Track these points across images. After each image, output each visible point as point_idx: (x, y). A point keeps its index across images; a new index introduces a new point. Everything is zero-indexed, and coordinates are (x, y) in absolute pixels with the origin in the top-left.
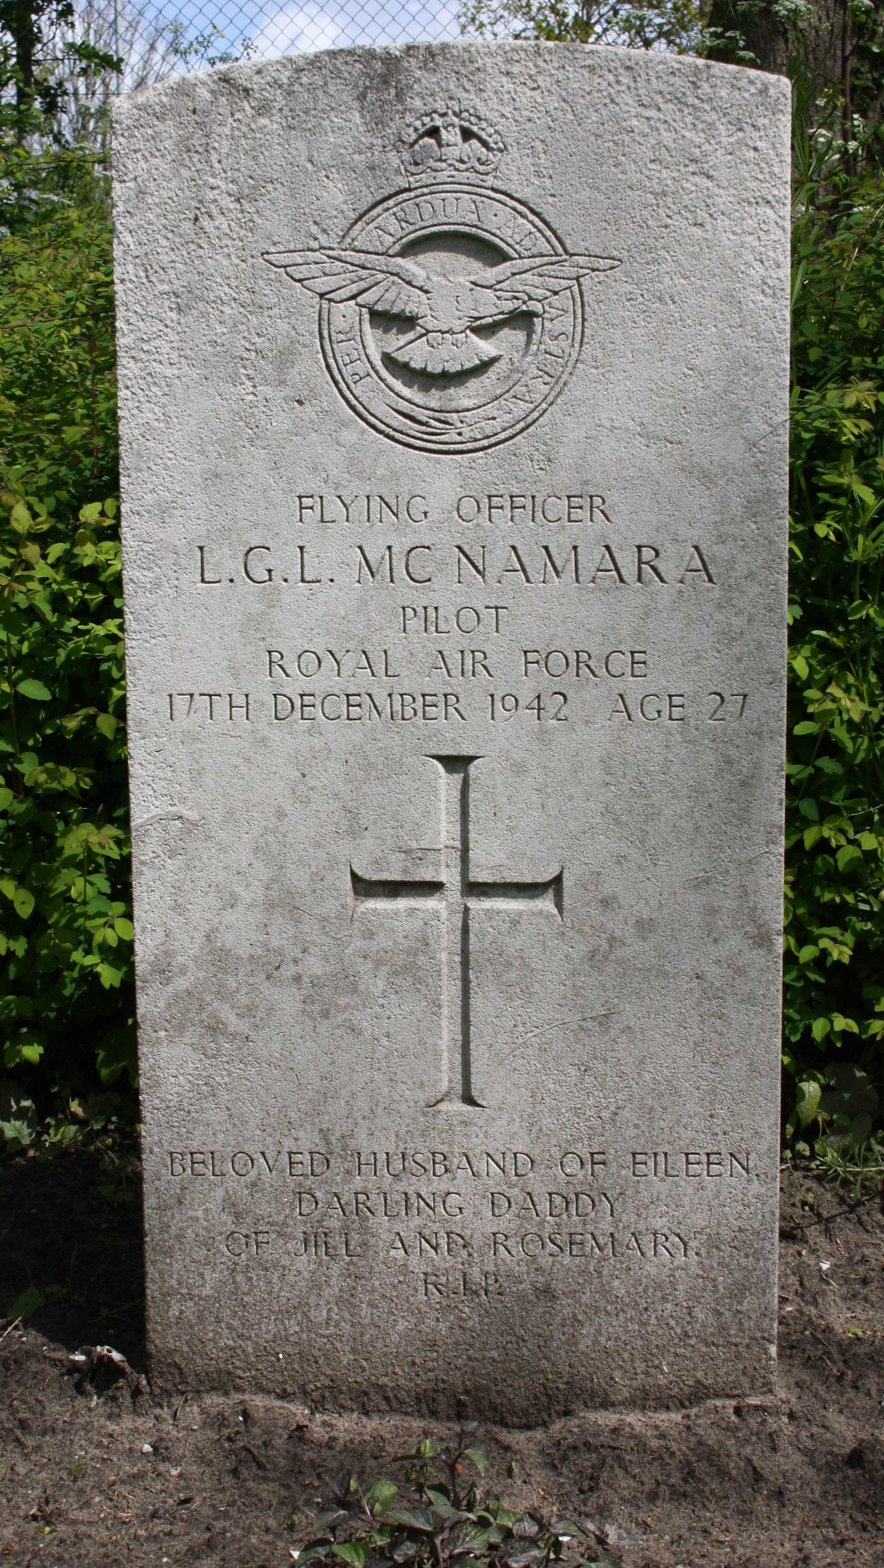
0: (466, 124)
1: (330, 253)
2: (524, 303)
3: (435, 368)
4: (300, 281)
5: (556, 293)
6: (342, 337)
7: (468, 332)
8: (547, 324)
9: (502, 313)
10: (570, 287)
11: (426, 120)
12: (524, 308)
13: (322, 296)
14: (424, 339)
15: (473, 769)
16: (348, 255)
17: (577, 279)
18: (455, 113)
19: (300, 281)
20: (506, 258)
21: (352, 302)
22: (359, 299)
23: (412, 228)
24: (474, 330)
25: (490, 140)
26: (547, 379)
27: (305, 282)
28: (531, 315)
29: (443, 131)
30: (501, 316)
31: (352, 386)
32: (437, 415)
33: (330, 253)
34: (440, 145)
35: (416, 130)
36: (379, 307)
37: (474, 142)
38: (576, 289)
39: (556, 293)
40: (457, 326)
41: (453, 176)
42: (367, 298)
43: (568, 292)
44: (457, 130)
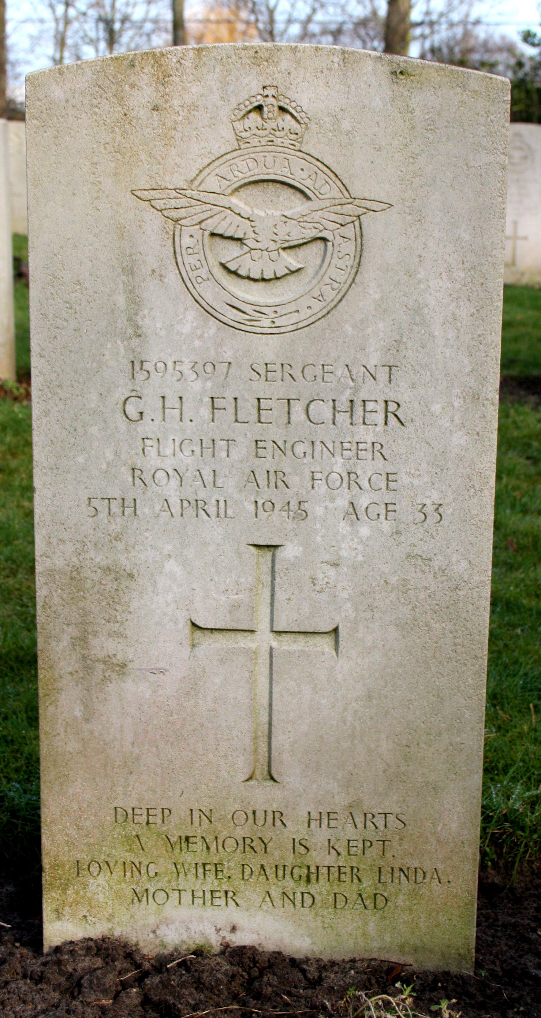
0: (282, 104)
1: (181, 192)
2: (321, 231)
3: (256, 275)
4: (161, 211)
5: (342, 225)
6: (190, 251)
7: (281, 251)
8: (337, 248)
9: (304, 238)
10: (353, 222)
11: (253, 100)
12: (320, 235)
13: (176, 221)
14: (249, 254)
15: (278, 552)
16: (195, 194)
17: (359, 216)
18: (273, 96)
19: (161, 211)
20: (308, 198)
21: (198, 227)
22: (203, 225)
23: (243, 176)
24: (284, 249)
25: (299, 118)
26: (336, 285)
27: (165, 213)
28: (324, 240)
29: (265, 109)
30: (305, 241)
31: (197, 286)
32: (258, 309)
33: (181, 192)
34: (262, 118)
35: (246, 106)
36: (215, 232)
37: (288, 117)
38: (357, 223)
39: (342, 225)
40: (273, 246)
41: (272, 141)
42: (210, 225)
43: (352, 225)
44: (276, 109)
